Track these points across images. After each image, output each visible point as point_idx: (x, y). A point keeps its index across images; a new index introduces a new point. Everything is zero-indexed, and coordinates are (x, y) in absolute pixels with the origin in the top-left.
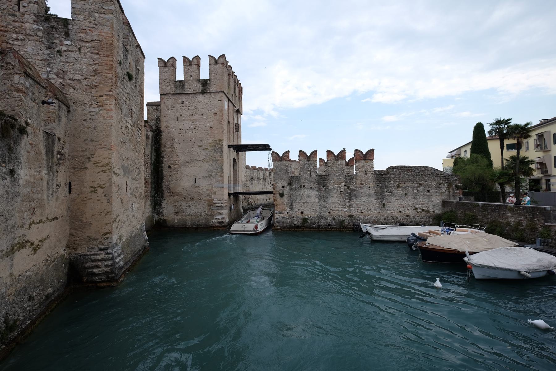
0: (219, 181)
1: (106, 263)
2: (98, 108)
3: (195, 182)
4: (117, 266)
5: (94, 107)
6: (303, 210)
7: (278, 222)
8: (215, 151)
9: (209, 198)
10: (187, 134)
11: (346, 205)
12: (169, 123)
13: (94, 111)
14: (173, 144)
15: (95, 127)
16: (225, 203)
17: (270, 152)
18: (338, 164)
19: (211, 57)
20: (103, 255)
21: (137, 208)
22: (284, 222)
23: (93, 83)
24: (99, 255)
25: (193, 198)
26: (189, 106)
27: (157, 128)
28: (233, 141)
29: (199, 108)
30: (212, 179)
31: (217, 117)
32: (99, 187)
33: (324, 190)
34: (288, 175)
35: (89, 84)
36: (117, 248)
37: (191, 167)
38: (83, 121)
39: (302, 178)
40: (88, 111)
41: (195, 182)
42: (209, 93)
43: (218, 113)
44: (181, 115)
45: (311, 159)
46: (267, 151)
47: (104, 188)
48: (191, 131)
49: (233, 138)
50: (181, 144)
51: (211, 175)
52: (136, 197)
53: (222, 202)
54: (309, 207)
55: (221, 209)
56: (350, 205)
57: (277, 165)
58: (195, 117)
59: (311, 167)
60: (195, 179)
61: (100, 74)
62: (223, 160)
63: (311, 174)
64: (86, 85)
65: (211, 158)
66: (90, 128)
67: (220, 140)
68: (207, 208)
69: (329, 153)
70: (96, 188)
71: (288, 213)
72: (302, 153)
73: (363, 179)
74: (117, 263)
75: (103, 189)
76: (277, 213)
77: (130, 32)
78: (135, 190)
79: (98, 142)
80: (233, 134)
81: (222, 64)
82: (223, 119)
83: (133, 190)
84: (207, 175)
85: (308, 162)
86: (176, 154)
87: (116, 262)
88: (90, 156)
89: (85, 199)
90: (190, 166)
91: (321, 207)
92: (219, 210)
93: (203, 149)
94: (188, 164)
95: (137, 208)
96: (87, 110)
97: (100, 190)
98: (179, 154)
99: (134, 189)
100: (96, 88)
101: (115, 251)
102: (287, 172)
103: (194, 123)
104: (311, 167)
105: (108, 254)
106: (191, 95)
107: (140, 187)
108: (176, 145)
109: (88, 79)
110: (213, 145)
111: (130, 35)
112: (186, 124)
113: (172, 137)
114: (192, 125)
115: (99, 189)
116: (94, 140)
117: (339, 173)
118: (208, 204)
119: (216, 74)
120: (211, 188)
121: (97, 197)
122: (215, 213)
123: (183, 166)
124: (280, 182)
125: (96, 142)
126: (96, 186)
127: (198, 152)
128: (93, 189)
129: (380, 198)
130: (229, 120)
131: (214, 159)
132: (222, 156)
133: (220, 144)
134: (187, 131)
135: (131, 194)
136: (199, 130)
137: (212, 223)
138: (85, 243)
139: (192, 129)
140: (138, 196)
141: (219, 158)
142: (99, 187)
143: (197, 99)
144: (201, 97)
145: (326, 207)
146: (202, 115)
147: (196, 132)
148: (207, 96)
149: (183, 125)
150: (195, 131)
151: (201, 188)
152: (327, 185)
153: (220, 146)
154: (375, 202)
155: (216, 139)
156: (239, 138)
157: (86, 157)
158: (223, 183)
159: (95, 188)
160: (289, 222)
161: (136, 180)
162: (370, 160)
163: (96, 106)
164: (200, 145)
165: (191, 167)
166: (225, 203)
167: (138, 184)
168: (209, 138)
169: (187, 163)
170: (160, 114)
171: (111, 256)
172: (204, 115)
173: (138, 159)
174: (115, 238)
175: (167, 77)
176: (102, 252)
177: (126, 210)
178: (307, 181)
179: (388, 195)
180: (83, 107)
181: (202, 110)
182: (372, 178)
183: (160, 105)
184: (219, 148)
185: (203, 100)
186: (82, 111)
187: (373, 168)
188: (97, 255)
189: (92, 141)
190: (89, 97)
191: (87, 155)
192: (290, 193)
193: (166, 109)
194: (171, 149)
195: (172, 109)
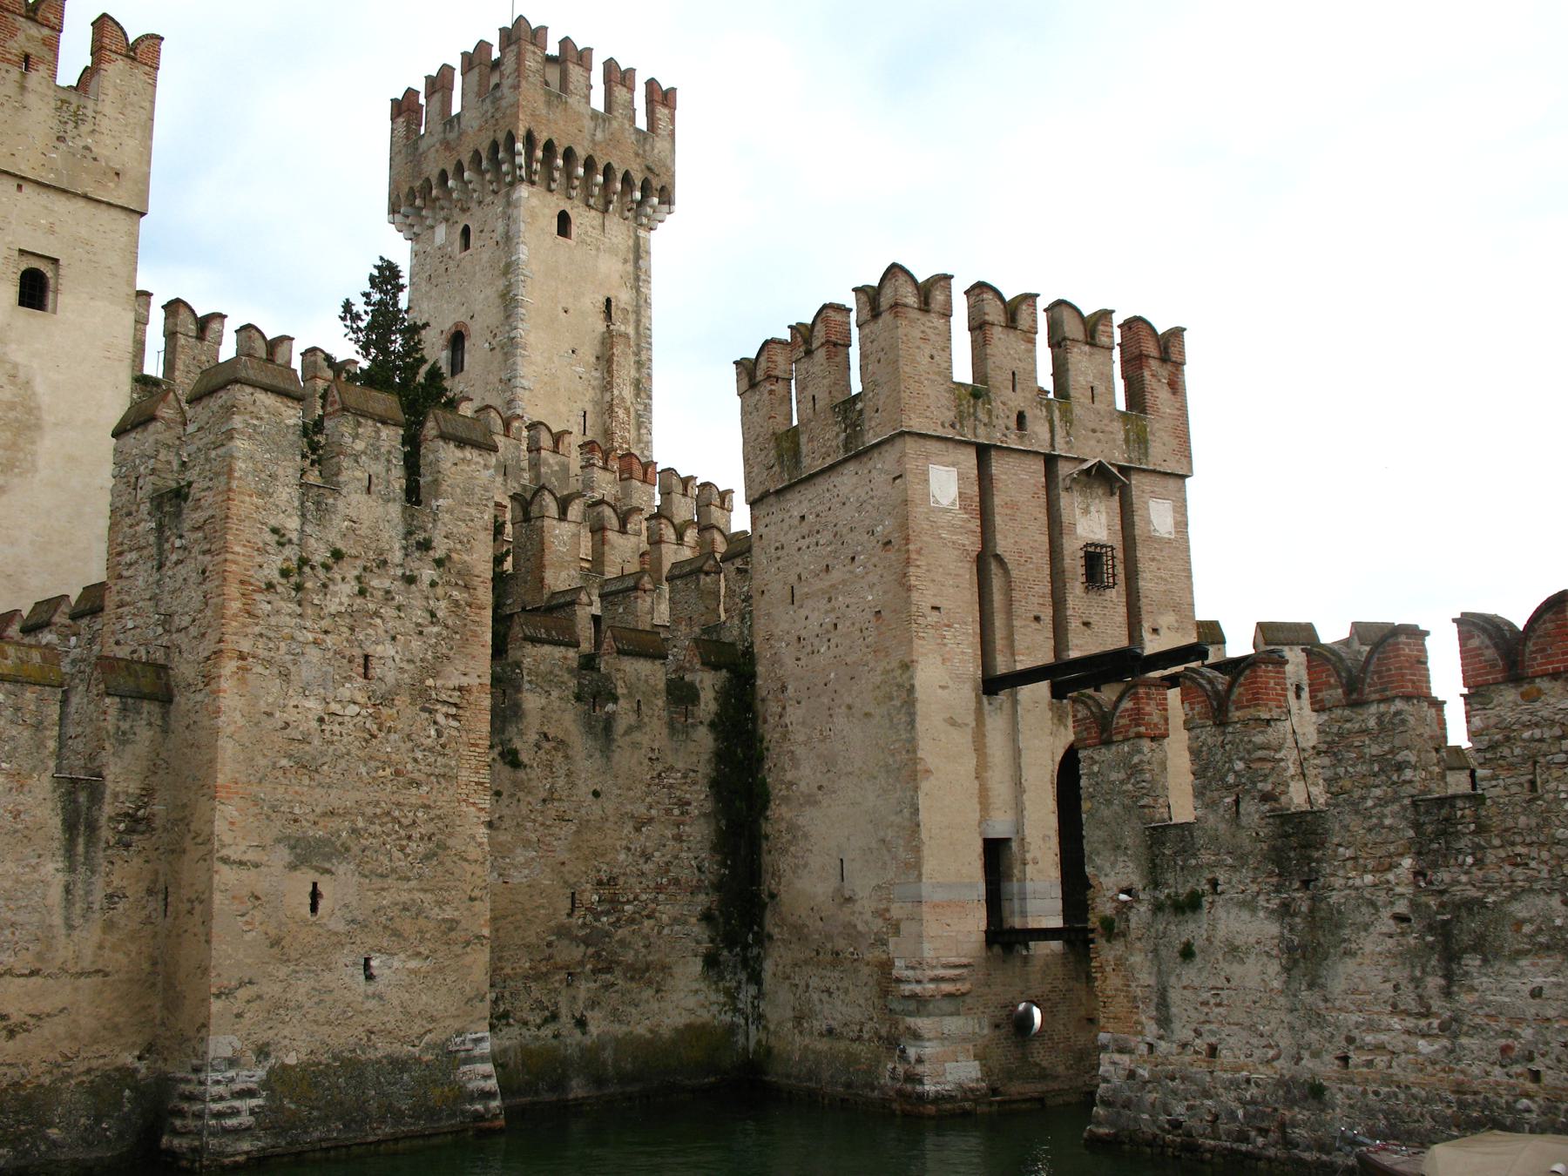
9: (877, 954)
10: (816, 657)
11: (1427, 1014)
14: (784, 708)
19: (860, 295)
26: (818, 532)
29: (845, 531)
31: (892, 555)
43: (895, 538)
45: (1235, 715)
50: (803, 703)
55: (917, 1013)
58: (836, 575)
59: (1239, 765)
63: (1243, 806)
67: (907, 666)
71: (1151, 1047)
81: (891, 307)
82: (908, 562)
84: (874, 845)
85: (1224, 733)
91: (1297, 1024)
92: (911, 1014)
98: (800, 751)
114: (827, 612)
117: (1378, 792)
118: (879, 984)
122: (901, 1027)
124: (1113, 865)
134: (816, 642)
141: (905, 756)
144: (847, 481)
151: (857, 907)
158: (920, 876)
175: (759, 429)
183: (749, 550)
185: (852, 491)
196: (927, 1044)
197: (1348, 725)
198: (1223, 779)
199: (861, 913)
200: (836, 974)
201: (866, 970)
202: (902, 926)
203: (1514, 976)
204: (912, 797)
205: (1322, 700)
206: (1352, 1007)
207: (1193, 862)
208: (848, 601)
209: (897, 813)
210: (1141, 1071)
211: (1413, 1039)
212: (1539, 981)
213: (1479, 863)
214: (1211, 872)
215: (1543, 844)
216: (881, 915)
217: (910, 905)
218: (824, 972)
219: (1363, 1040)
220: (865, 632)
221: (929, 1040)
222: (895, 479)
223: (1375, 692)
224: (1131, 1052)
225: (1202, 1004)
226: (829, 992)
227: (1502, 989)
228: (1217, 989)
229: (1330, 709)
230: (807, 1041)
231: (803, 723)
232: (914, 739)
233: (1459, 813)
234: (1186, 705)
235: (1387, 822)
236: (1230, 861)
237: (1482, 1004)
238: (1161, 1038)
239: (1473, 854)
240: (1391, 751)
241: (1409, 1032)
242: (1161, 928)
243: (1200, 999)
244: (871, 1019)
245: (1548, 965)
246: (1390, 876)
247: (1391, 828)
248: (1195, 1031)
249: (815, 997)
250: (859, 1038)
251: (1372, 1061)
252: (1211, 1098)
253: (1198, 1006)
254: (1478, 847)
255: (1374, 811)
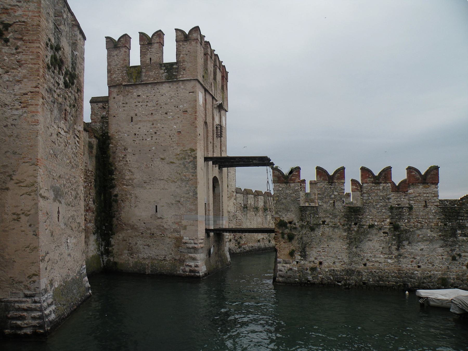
0: (191, 211)
1: (33, 315)
2: (21, 110)
3: (156, 211)
4: (47, 320)
5: (17, 109)
6: (322, 259)
7: (281, 276)
8: (185, 166)
9: (176, 235)
10: (144, 141)
11: (392, 253)
12: (120, 126)
13: (17, 113)
14: (125, 155)
15: (18, 135)
16: (200, 243)
17: (269, 168)
18: (379, 189)
20: (28, 304)
21: (74, 244)
22: (291, 276)
23: (16, 77)
24: (25, 303)
25: (153, 234)
26: (147, 102)
27: (104, 134)
28: (213, 152)
29: (162, 104)
30: (180, 208)
31: (188, 115)
32: (23, 213)
33: (355, 229)
34: (299, 204)
35: (11, 80)
36: (46, 296)
37: (151, 189)
38: (4, 128)
39: (320, 210)
40: (10, 114)
41: (156, 211)
42: (175, 81)
43: (189, 110)
44: (136, 115)
45: (335, 181)
46: (265, 168)
47: (29, 215)
48: (150, 136)
49: (213, 147)
51: (179, 202)
52: (72, 229)
53: (196, 241)
54: (331, 254)
56: (400, 255)
57: (280, 189)
59: (336, 193)
60: (156, 206)
61: (25, 65)
62: (196, 179)
63: (336, 204)
64: (7, 81)
65: (179, 176)
66: (12, 136)
67: (193, 150)
68: (173, 249)
69: (365, 171)
70: (19, 215)
71: (297, 262)
72: (321, 171)
73: (421, 213)
74: (48, 316)
75: (28, 217)
76: (280, 262)
77: (64, 7)
78: (71, 220)
79: (21, 154)
80: (213, 141)
82: (196, 119)
83: (68, 219)
84: (174, 202)
86: (130, 170)
87: (45, 314)
88: (12, 173)
89: (7, 229)
90: (148, 187)
91: (351, 256)
92: (191, 253)
93: (168, 164)
94: (145, 185)
95: (74, 244)
96: (8, 113)
97: (23, 218)
98: (133, 170)
99: (69, 218)
100: (19, 83)
101: (44, 299)
102: (296, 200)
103: (155, 125)
104: (336, 193)
105: (35, 302)
106: (150, 86)
107: (78, 216)
108: (129, 158)
109: (9, 73)
110: (181, 156)
111: (64, 11)
112: (144, 126)
113: (123, 146)
114: (151, 128)
115: (22, 217)
116: (16, 152)
117: (381, 204)
118: (175, 244)
119: (187, 55)
120: (179, 220)
121: (21, 227)
123: (139, 187)
125: (19, 154)
126: (19, 212)
127: (159, 167)
128: (15, 217)
129: (450, 245)
130: (206, 119)
131: (184, 178)
132: (195, 174)
133: (191, 156)
134: (145, 137)
135: (65, 224)
136: (161, 135)
137: (181, 272)
138: (8, 286)
139: (151, 134)
140: (75, 228)
141: (191, 177)
142: (23, 213)
143: (158, 91)
144: (165, 89)
145: (359, 256)
146: (166, 113)
147: (158, 138)
148: (174, 86)
149: (140, 128)
150: (156, 137)
152: (361, 221)
153: (192, 159)
154: (440, 250)
155: (186, 149)
156: (222, 146)
157: (7, 174)
158: (197, 213)
159: (18, 215)
160: (299, 276)
161: (72, 206)
162: (433, 184)
163: (19, 107)
164: (163, 157)
165: (151, 189)
166: (200, 243)
167: (75, 211)
168: (176, 147)
169: (145, 183)
170: (108, 114)
171: (39, 305)
172: (168, 113)
173: (75, 177)
174: (43, 283)
176: (28, 299)
177: (58, 246)
178: (328, 215)
179: (463, 241)
180: (4, 109)
181: (166, 106)
182: (435, 212)
184: (191, 162)
186: (3, 114)
187: (438, 196)
188: (21, 302)
189: (15, 153)
190: (10, 96)
191: (8, 172)
192: (301, 233)
193: (116, 107)
194: (121, 163)
195: (124, 107)
196: (199, 262)
197: (374, 187)
198: (330, 196)
199: (166, 222)
200: (152, 240)
201: (168, 240)
202: (187, 227)
203: (416, 246)
204: (195, 190)
205: (367, 181)
206: (369, 253)
207: (318, 216)
208: (163, 126)
209: (186, 194)
210: (294, 268)
211: (387, 259)
212: (423, 247)
213: (409, 222)
214: (324, 219)
215: (426, 219)
216: (176, 224)
217: (192, 221)
218: (145, 240)
219: (372, 260)
220: (172, 137)
221: (199, 260)
222: (189, 92)
223: (383, 181)
224: (290, 263)
225: (318, 251)
226: (148, 246)
227: (413, 249)
228: (323, 248)
229: (368, 183)
230: (136, 260)
231: (137, 161)
232: (196, 172)
233: (404, 211)
234: (319, 176)
235: (383, 211)
236: (331, 217)
237: (407, 252)
238: (302, 260)
239: (407, 220)
240: (386, 195)
241: (385, 258)
242: (304, 232)
243: (318, 250)
244: (171, 254)
245: (426, 244)
246: (383, 223)
247: (384, 212)
248: (315, 258)
249: (141, 247)
250: (164, 260)
251: (374, 264)
252: (321, 274)
253: (316, 252)
254: (409, 218)
255: (379, 208)
